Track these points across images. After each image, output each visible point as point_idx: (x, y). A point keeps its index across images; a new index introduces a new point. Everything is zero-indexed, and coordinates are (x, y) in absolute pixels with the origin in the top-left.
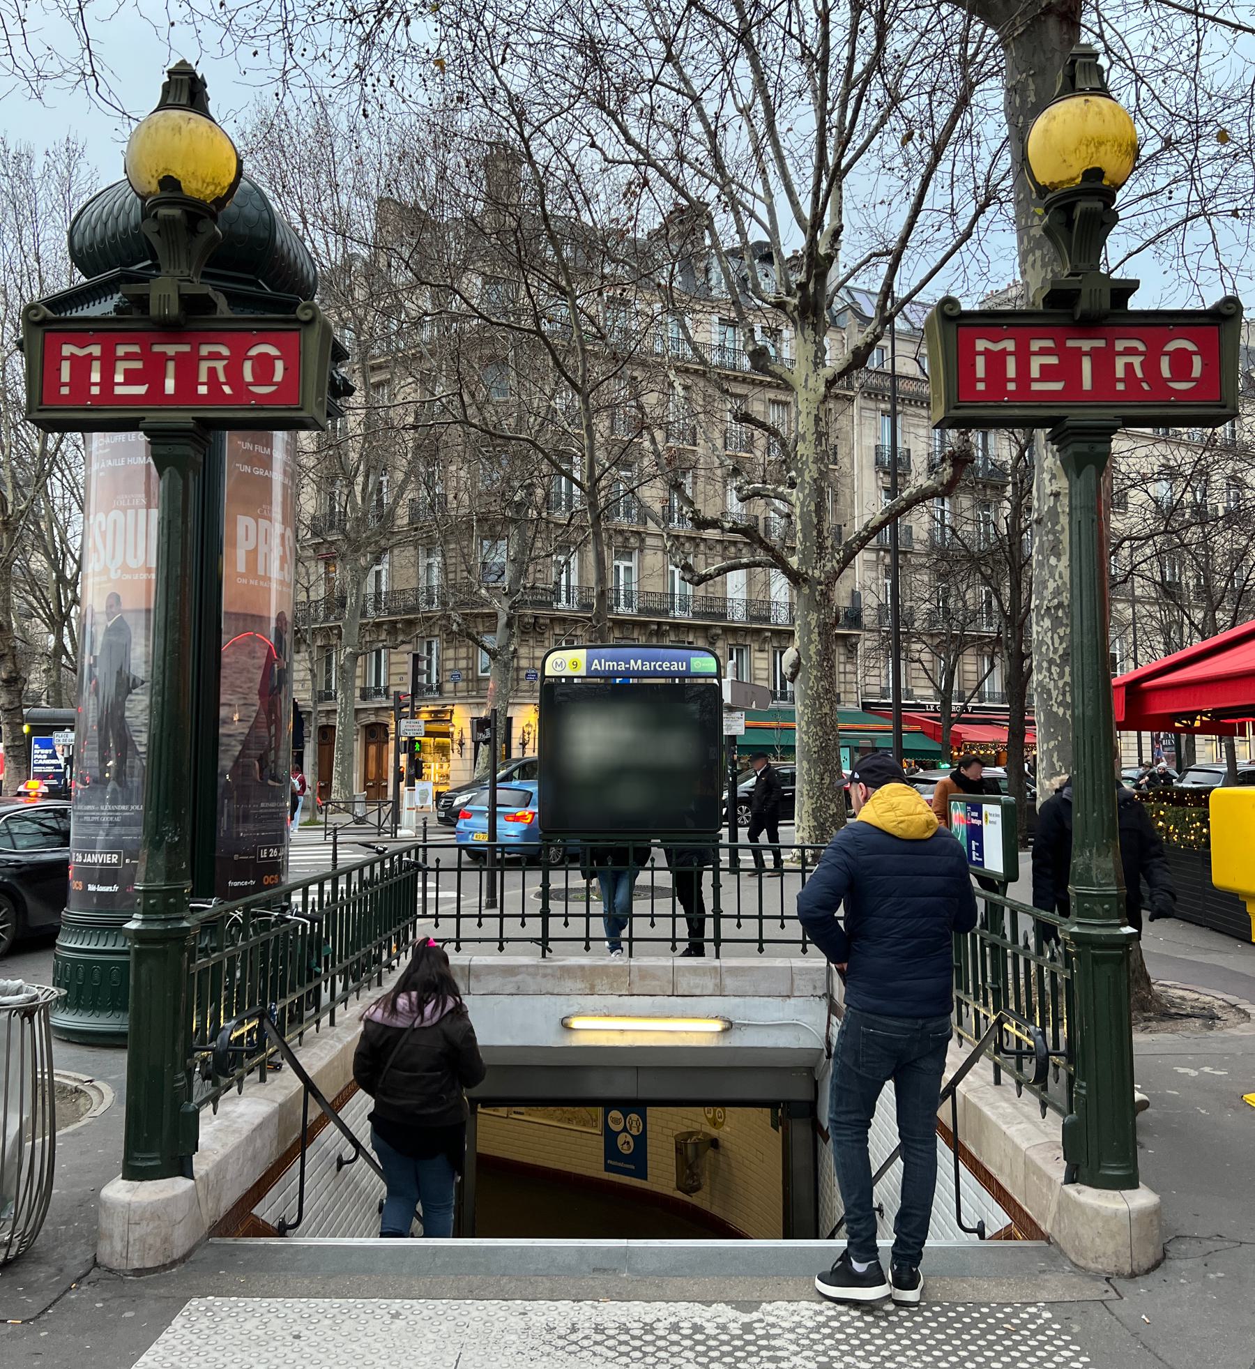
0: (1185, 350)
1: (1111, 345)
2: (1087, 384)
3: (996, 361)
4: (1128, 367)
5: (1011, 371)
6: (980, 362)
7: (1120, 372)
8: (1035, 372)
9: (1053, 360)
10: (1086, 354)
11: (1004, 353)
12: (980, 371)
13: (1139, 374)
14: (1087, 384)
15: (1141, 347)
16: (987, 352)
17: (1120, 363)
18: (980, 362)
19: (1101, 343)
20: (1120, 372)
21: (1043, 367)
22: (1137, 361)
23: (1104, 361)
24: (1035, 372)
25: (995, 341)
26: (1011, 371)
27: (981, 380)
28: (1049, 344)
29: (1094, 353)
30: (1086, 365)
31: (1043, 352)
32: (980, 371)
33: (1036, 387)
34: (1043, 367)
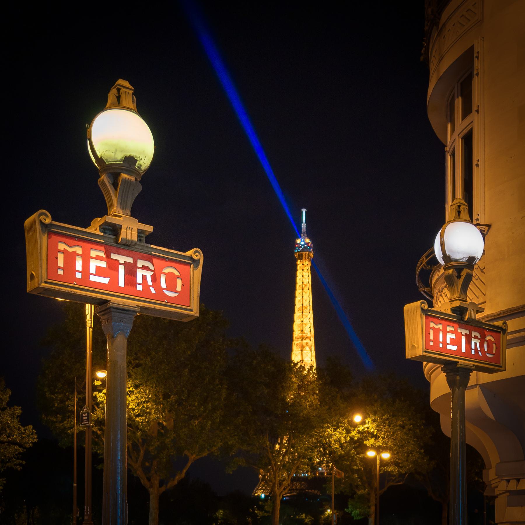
0: (173, 274)
1: (135, 262)
3: (70, 258)
4: (144, 277)
5: (79, 266)
6: (61, 257)
7: (139, 280)
8: (93, 270)
9: (104, 264)
10: (122, 264)
12: (61, 263)
16: (64, 252)
17: (140, 273)
19: (130, 260)
22: (149, 275)
23: (131, 271)
25: (70, 246)
27: (61, 268)
29: (126, 264)
30: (122, 270)
31: (98, 258)
32: (61, 263)
33: (93, 278)
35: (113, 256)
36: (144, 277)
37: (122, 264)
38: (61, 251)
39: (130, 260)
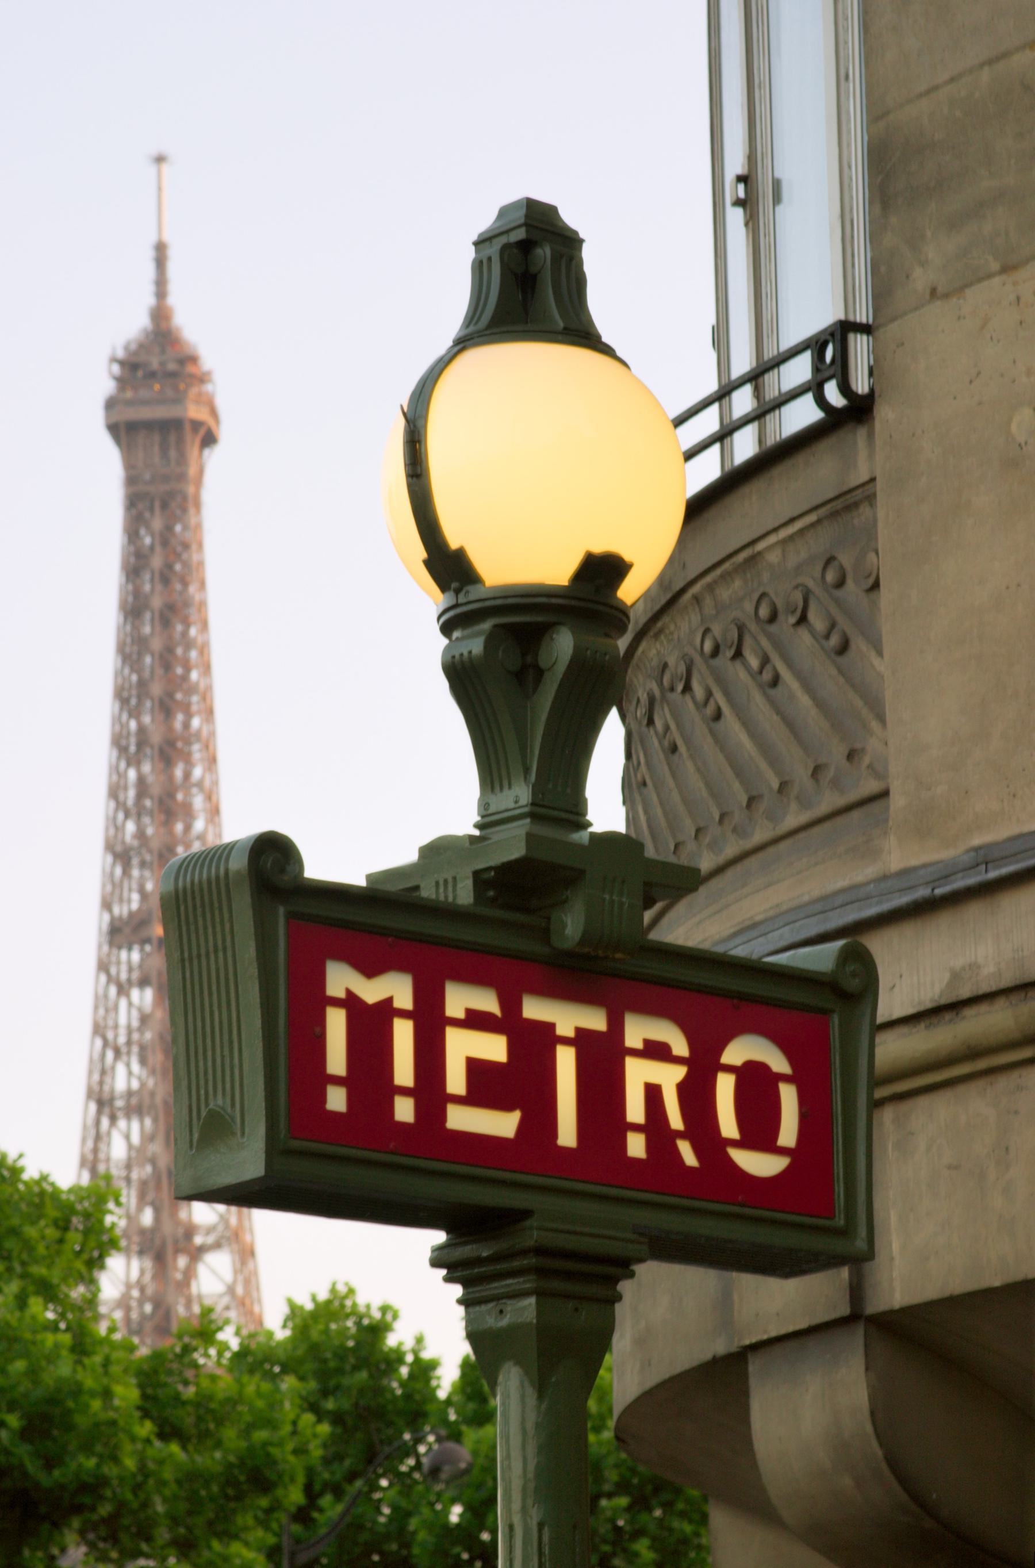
2: (567, 1134)
4: (653, 1094)
5: (404, 1072)
7: (635, 1110)
8: (456, 1081)
10: (566, 1041)
11: (386, 1010)
12: (337, 1062)
13: (676, 1121)
14: (567, 1134)
15: (680, 1047)
16: (351, 1002)
18: (336, 1022)
19: (596, 1021)
20: (635, 1110)
21: (475, 1067)
24: (456, 1081)
26: (404, 1072)
28: (487, 1002)
29: (582, 1039)
31: (475, 1021)
32: (337, 1062)
34: (475, 1067)
35: (534, 1009)
36: (653, 1094)
37: (566, 1041)
38: (336, 1002)
39: (596, 1021)
